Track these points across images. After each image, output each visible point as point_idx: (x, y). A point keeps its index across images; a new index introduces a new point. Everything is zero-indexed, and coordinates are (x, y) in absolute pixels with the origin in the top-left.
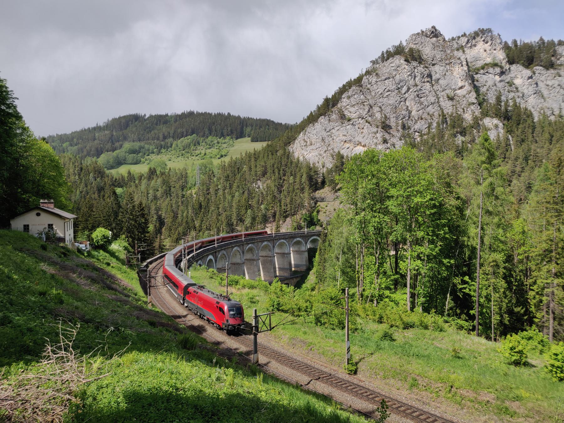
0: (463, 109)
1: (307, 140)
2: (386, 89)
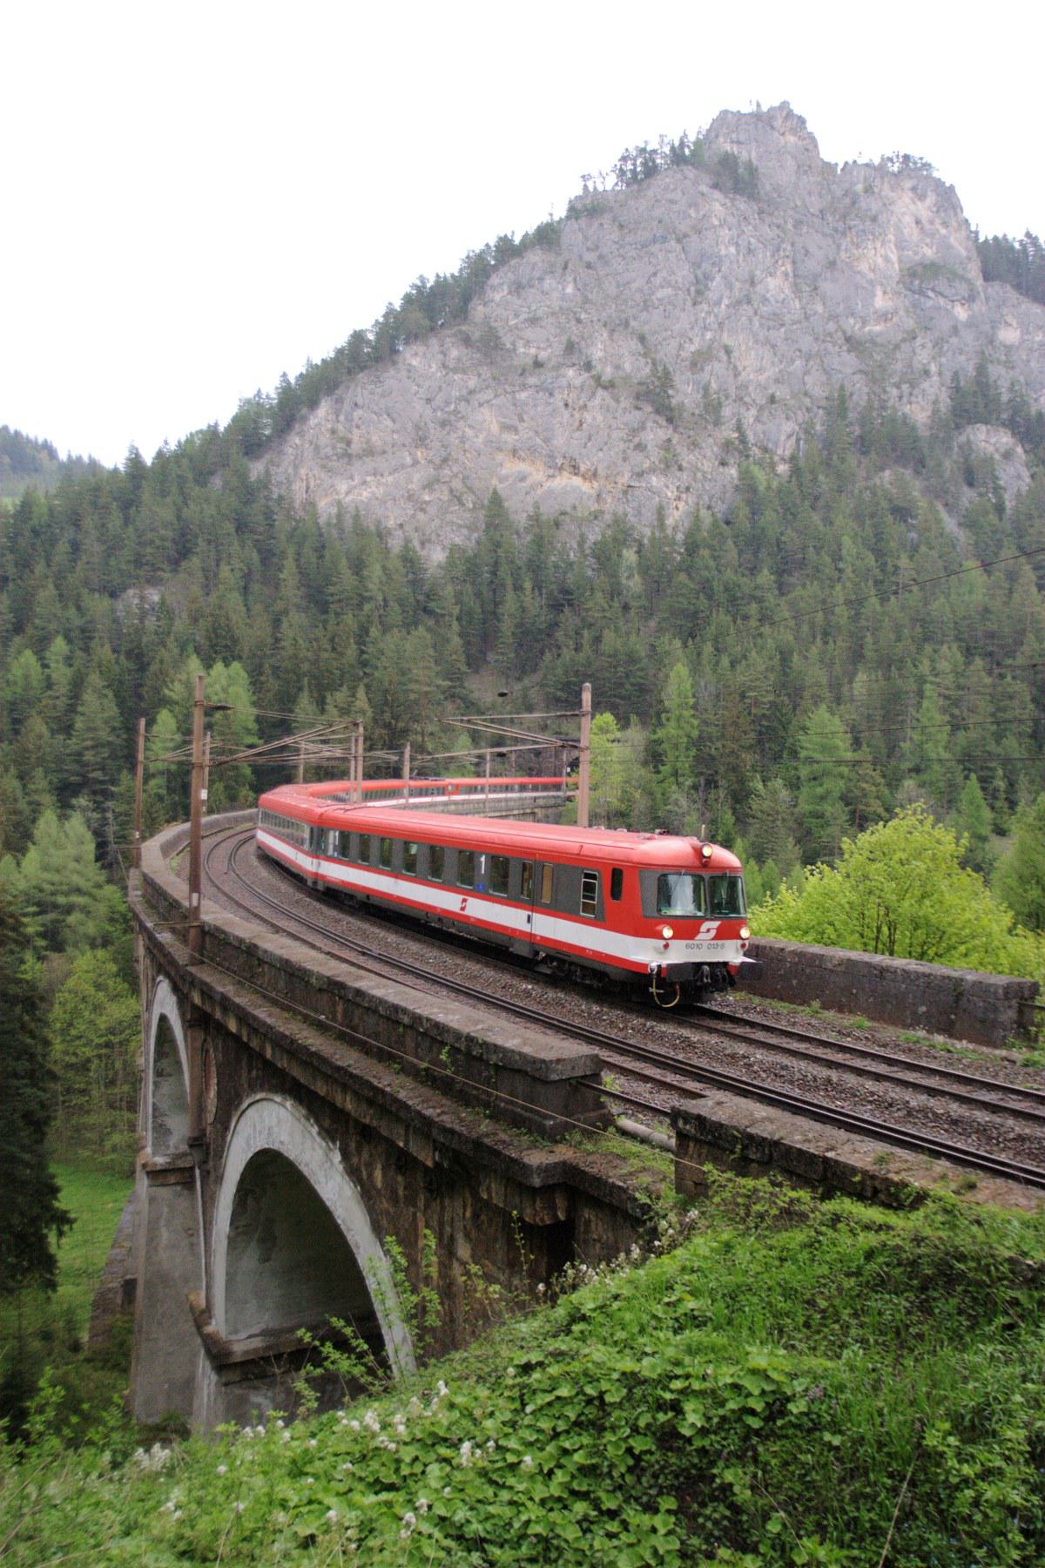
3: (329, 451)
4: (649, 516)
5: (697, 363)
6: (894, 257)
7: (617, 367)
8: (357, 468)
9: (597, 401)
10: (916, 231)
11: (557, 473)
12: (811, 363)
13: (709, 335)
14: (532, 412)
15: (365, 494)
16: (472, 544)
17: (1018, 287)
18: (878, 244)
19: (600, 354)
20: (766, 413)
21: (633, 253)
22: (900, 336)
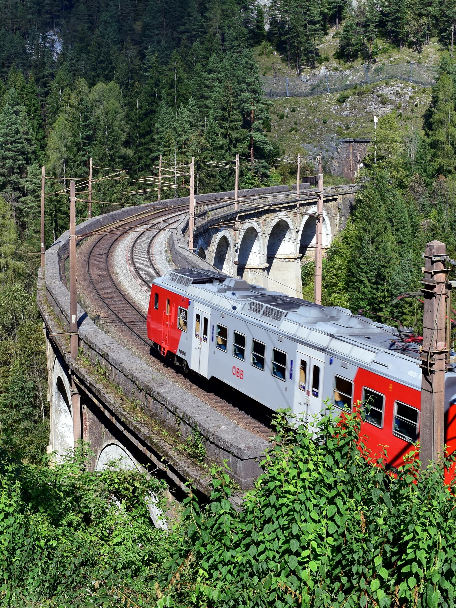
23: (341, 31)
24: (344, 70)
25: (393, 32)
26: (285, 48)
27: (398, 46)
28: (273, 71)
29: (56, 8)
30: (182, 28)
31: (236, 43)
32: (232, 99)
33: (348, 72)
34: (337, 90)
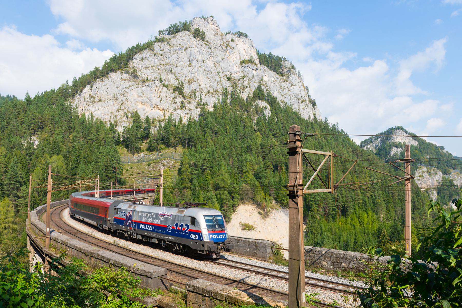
0: (240, 90)
1: (94, 96)
2: (179, 58)
3: (89, 100)
4: (177, 120)
5: (190, 81)
6: (239, 58)
7: (169, 82)
8: (98, 105)
9: (163, 91)
10: (244, 51)
11: (153, 108)
12: (218, 83)
13: (193, 75)
14: (146, 92)
15: (99, 112)
16: (130, 127)
17: (268, 67)
18: (235, 54)
19: (164, 78)
20: (207, 95)
21: (173, 52)
22: (240, 78)
23: (148, 142)
24: (150, 155)
25: (166, 142)
26: (128, 147)
27: (168, 147)
28: (123, 155)
29: (36, 128)
30: (89, 138)
31: (110, 144)
32: (109, 163)
33: (151, 155)
34: (147, 161)
